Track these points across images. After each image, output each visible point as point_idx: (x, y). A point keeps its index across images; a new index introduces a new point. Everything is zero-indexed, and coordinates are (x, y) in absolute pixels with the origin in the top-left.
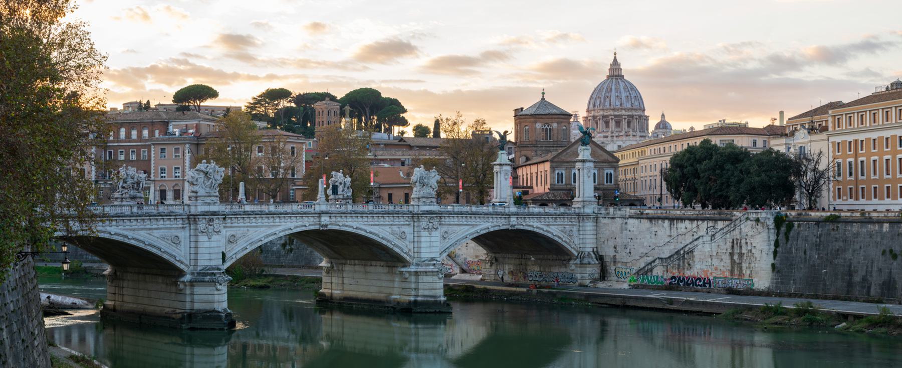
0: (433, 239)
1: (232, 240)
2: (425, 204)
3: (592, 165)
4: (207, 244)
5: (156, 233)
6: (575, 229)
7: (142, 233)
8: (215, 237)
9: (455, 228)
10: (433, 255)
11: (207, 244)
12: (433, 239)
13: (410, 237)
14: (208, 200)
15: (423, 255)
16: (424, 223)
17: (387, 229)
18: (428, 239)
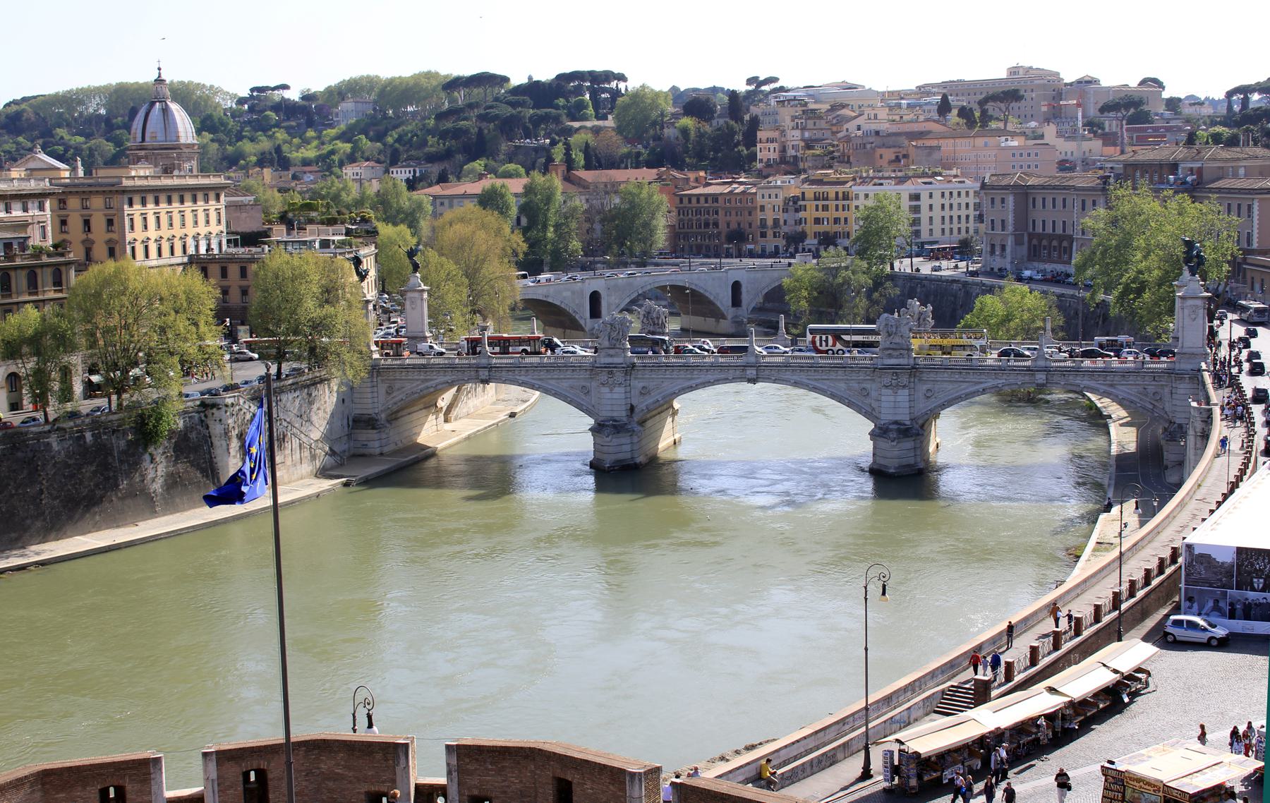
0: (899, 398)
1: (644, 392)
2: (890, 356)
3: (1199, 303)
4: (609, 396)
5: (565, 384)
6: (1167, 390)
7: (553, 382)
8: (617, 389)
9: (945, 385)
10: (898, 418)
11: (609, 396)
12: (899, 398)
13: (874, 394)
14: (612, 352)
15: (883, 417)
16: (887, 380)
17: (842, 385)
18: (892, 399)
